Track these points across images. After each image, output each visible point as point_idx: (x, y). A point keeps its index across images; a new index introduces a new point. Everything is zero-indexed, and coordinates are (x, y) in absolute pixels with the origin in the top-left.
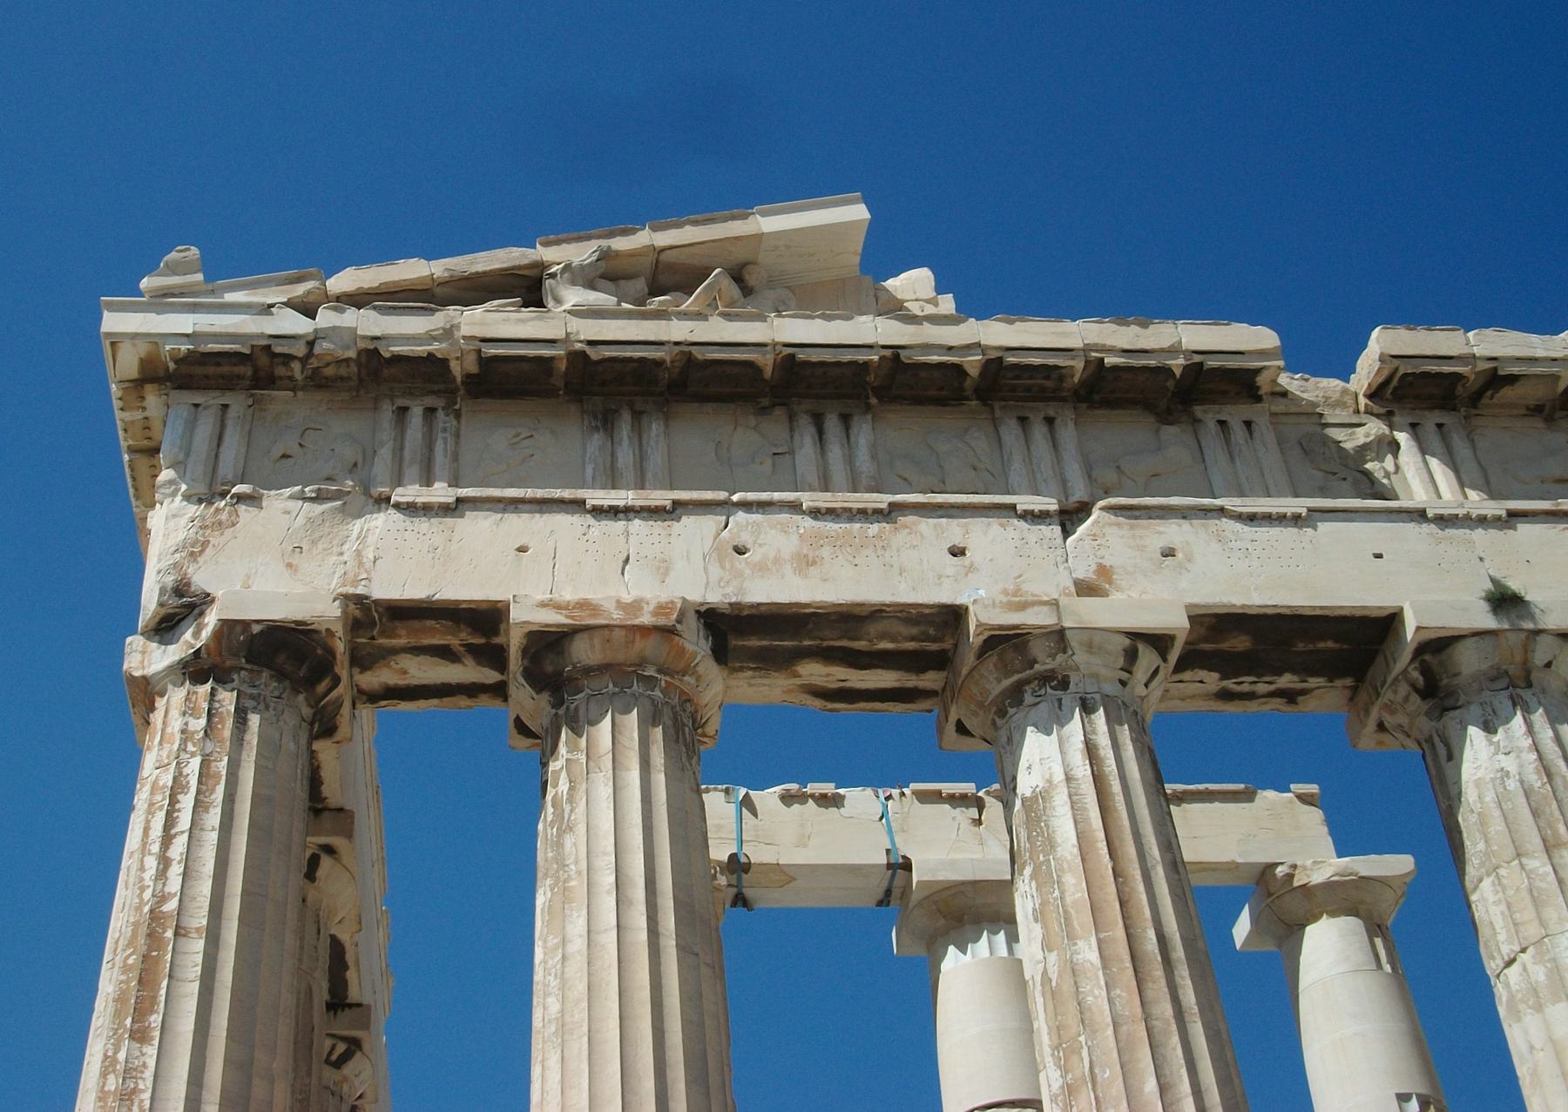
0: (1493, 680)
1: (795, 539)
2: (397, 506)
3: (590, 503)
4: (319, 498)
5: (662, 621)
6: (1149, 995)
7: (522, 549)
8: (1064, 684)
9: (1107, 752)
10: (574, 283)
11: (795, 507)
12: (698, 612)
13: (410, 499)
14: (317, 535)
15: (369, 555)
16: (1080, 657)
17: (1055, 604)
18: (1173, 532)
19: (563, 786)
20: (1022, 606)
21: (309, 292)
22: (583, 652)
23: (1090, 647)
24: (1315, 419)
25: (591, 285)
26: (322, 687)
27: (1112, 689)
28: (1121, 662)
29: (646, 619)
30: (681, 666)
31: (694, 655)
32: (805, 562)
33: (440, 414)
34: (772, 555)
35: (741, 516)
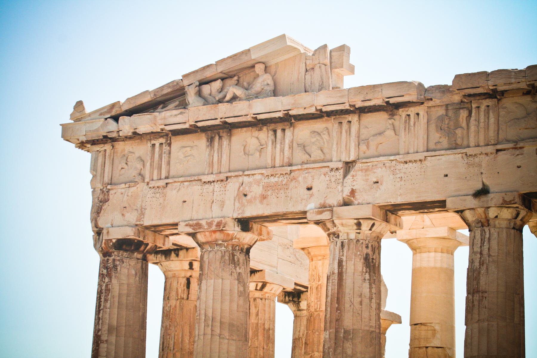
0: (478, 223)
1: (261, 187)
3: (203, 180)
7: (185, 202)
8: (338, 237)
9: (344, 263)
16: (341, 228)
18: (379, 173)
20: (321, 213)
22: (201, 238)
23: (342, 225)
26: (142, 248)
27: (353, 236)
28: (355, 227)
29: (214, 228)
30: (230, 238)
31: (233, 234)
33: (164, 145)
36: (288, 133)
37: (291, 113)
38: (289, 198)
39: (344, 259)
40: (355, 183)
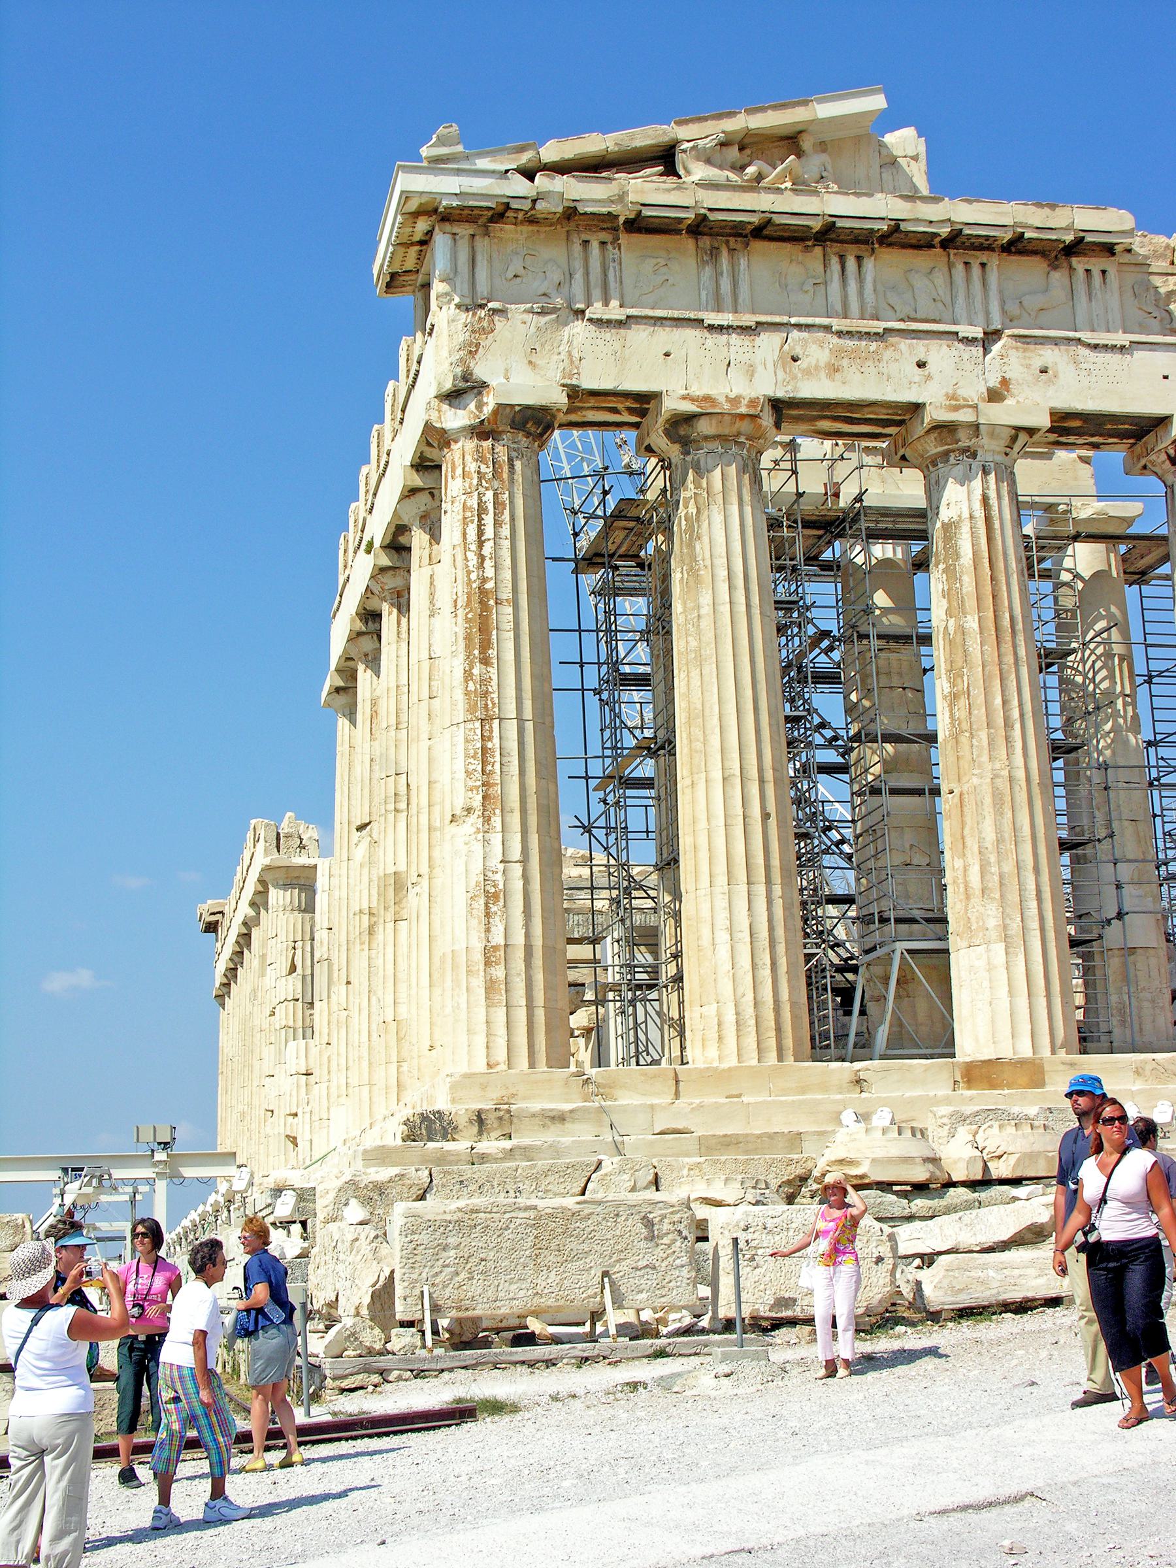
1: (827, 351)
2: (590, 320)
3: (707, 322)
4: (543, 312)
5: (752, 412)
6: (1003, 650)
7: (667, 355)
8: (974, 455)
9: (993, 502)
10: (698, 159)
11: (827, 328)
12: (769, 400)
13: (599, 316)
14: (543, 340)
15: (576, 355)
16: (985, 441)
17: (975, 407)
18: (1049, 355)
19: (692, 510)
20: (956, 408)
21: (529, 160)
23: (992, 435)
24: (1144, 269)
25: (708, 161)
29: (743, 410)
32: (834, 370)
33: (610, 247)
34: (814, 363)
35: (795, 334)
36: (869, 264)
37: (904, 226)
38: (885, 377)
39: (992, 494)
40: (1006, 368)
